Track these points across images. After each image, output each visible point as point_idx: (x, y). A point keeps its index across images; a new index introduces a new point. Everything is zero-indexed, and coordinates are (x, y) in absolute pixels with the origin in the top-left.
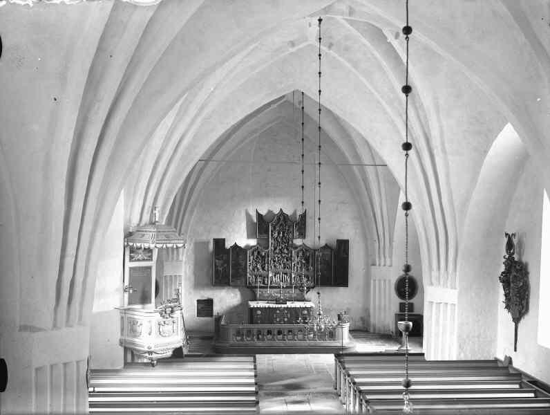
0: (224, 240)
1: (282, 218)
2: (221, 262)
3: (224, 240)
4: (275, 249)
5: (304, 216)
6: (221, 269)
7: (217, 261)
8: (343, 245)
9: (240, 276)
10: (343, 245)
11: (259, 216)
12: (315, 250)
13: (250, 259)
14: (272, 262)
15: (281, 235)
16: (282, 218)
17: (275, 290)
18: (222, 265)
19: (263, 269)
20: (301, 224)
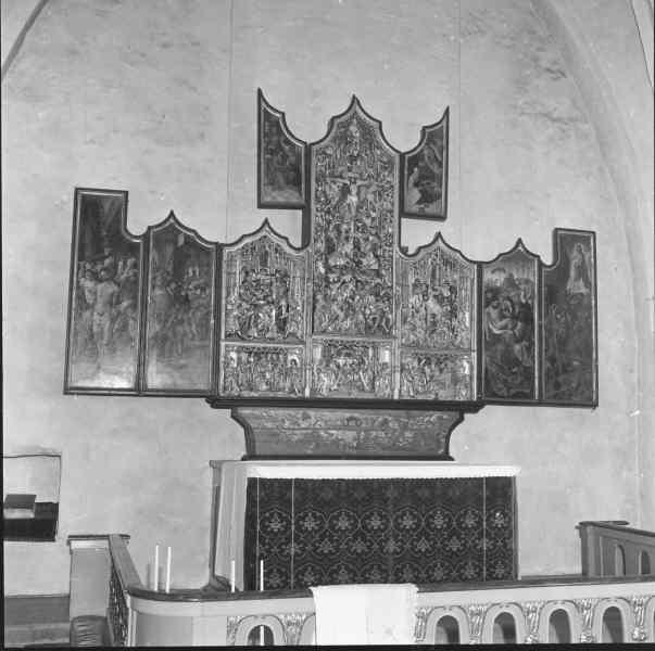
0: (121, 201)
3: (121, 201)
4: (331, 249)
5: (435, 136)
7: (88, 284)
12: (480, 265)
17: (327, 414)
18: (113, 302)
19: (282, 324)
20: (424, 175)
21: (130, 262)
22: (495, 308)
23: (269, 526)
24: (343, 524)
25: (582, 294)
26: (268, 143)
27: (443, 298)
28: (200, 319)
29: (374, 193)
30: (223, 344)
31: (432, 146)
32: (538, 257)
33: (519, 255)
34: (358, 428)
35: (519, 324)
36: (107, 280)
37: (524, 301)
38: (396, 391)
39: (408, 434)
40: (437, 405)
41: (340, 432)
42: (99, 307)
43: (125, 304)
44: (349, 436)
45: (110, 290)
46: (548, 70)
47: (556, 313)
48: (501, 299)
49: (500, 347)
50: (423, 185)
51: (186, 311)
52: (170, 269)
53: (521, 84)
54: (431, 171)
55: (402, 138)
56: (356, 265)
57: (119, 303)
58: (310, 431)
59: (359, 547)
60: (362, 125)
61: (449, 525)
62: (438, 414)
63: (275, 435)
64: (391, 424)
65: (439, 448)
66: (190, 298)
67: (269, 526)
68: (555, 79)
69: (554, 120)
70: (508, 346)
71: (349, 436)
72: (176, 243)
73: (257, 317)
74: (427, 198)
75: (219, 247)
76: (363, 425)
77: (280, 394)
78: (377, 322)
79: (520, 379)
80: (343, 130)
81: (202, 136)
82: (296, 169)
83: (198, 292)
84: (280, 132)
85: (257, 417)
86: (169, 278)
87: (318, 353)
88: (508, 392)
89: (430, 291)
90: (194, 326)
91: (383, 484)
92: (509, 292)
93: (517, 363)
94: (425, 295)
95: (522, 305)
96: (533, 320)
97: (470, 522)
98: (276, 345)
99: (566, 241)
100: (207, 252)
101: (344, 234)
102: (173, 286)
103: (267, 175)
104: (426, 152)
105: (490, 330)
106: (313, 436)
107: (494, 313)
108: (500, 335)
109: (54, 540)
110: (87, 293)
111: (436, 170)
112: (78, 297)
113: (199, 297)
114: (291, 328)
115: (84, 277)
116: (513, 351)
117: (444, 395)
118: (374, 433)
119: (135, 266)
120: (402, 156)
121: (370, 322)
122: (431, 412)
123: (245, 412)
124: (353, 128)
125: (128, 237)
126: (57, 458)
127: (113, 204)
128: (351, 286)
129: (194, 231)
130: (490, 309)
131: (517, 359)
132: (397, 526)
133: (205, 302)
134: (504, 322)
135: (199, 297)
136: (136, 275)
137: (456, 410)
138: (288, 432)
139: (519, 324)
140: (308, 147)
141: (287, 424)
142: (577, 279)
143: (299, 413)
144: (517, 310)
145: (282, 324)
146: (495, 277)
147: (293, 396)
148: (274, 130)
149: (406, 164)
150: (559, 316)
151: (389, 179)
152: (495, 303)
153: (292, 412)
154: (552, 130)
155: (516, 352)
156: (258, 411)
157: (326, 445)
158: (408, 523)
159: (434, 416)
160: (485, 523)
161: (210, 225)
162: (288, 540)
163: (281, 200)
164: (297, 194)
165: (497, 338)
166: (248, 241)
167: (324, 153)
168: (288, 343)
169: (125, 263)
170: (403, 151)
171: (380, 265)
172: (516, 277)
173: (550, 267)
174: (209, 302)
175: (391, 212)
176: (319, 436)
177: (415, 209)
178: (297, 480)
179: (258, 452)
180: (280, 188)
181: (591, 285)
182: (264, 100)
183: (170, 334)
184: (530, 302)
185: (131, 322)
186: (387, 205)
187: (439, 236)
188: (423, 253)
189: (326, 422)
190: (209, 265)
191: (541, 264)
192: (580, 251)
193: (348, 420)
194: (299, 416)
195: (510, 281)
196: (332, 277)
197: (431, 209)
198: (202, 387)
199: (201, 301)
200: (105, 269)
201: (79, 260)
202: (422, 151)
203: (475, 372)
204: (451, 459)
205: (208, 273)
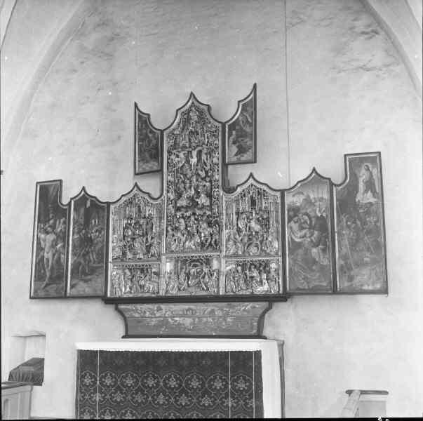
1: (194, 116)
2: (51, 237)
5: (249, 106)
6: (50, 256)
7: (43, 236)
8: (364, 165)
9: (93, 271)
10: (364, 165)
11: (143, 121)
12: (282, 192)
13: (116, 223)
14: (171, 232)
15: (194, 160)
16: (194, 116)
18: (54, 245)
19: (148, 248)
20: (243, 133)
21: (62, 221)
22: (295, 222)
23: (237, 386)
24: (129, 382)
25: (370, 203)
26: (140, 135)
27: (263, 219)
28: (98, 251)
29: (206, 154)
30: (110, 265)
31: (245, 114)
32: (329, 179)
33: (316, 178)
34: (193, 316)
35: (316, 233)
36: (51, 233)
37: (319, 215)
38: (221, 289)
39: (229, 320)
40: (253, 298)
41: (182, 318)
42: (46, 250)
43: (59, 246)
44: (188, 321)
45: (52, 239)
46: (363, 33)
47: (347, 222)
48: (300, 215)
49: (301, 251)
50: (239, 142)
51: (91, 246)
52: (82, 221)
53: (339, 50)
54: (244, 131)
55: (228, 111)
56: (193, 203)
57: (56, 245)
58: (162, 319)
59: (139, 398)
60: (198, 109)
61: (180, 385)
62: (251, 304)
63: (139, 322)
64: (216, 313)
65: (252, 328)
66: (93, 237)
67: (177, 384)
68: (371, 38)
69: (368, 70)
70: (307, 251)
71: (188, 321)
72: (86, 206)
73: (131, 248)
74: (242, 150)
75: (108, 204)
76: (198, 314)
77: (146, 295)
78: (209, 241)
79: (318, 274)
80: (186, 116)
81: (119, 138)
82: (157, 148)
83: (97, 234)
84: (147, 126)
85: (129, 310)
86: (82, 227)
87: (168, 267)
88: (308, 283)
89: (254, 215)
90: (95, 256)
91: (224, 355)
92: (307, 209)
93: (315, 262)
94: (249, 220)
95: (318, 218)
96: (327, 229)
97: (218, 385)
98: (143, 263)
99: (355, 162)
100: (102, 208)
101: (188, 185)
102: (84, 231)
103: (140, 154)
104: (241, 118)
105: (292, 239)
106: (164, 322)
107: (295, 226)
108: (300, 243)
109: (41, 385)
110: (42, 242)
111: (248, 129)
112: (37, 243)
113: (98, 237)
114: (153, 250)
115: (40, 232)
116: (310, 252)
117: (261, 289)
118: (205, 319)
119: (64, 223)
120: (224, 125)
121: (204, 242)
122: (246, 303)
123: (122, 307)
124: (190, 114)
125: (99, 204)
126: (41, 339)
127: (54, 188)
128: (192, 218)
129: (95, 197)
130: (292, 224)
131: (314, 260)
132: (165, 384)
133: (101, 239)
134: (304, 232)
135: (98, 237)
136: (65, 228)
137: (266, 301)
138: (149, 319)
139: (316, 233)
140: (162, 132)
141: (147, 314)
142: (366, 191)
143: (154, 307)
144: (313, 223)
145: (148, 248)
146: (295, 199)
147: (153, 295)
148: (144, 126)
149: (227, 129)
150: (349, 223)
151: (215, 142)
152: (296, 219)
153: (150, 306)
154: (366, 77)
155: (313, 255)
156: (129, 307)
157: (172, 328)
158: (173, 383)
159: (249, 305)
160: (98, 382)
161: (101, 192)
162: (95, 392)
163: (148, 169)
164: (157, 164)
165: (299, 245)
166: (124, 199)
167: (173, 134)
168: (148, 261)
169: (60, 222)
170: (224, 121)
171: (211, 202)
172: (312, 197)
173: (340, 185)
174: (103, 241)
175: (218, 165)
176: (168, 322)
177: (234, 159)
178: (100, 351)
179: (129, 333)
180: (147, 162)
181: (381, 196)
182: (138, 109)
183: (82, 261)
184: (324, 215)
185: (62, 256)
186: (215, 160)
187: (251, 175)
188: (239, 190)
189: (172, 313)
190: (103, 217)
191: (332, 185)
192: (368, 169)
193: (187, 311)
194: (156, 308)
195: (308, 201)
196: (179, 214)
197: (247, 156)
198: (100, 293)
199: (98, 239)
200: (49, 227)
201: (38, 223)
202: (238, 118)
203: (281, 272)
204: (265, 338)
205: (103, 222)
